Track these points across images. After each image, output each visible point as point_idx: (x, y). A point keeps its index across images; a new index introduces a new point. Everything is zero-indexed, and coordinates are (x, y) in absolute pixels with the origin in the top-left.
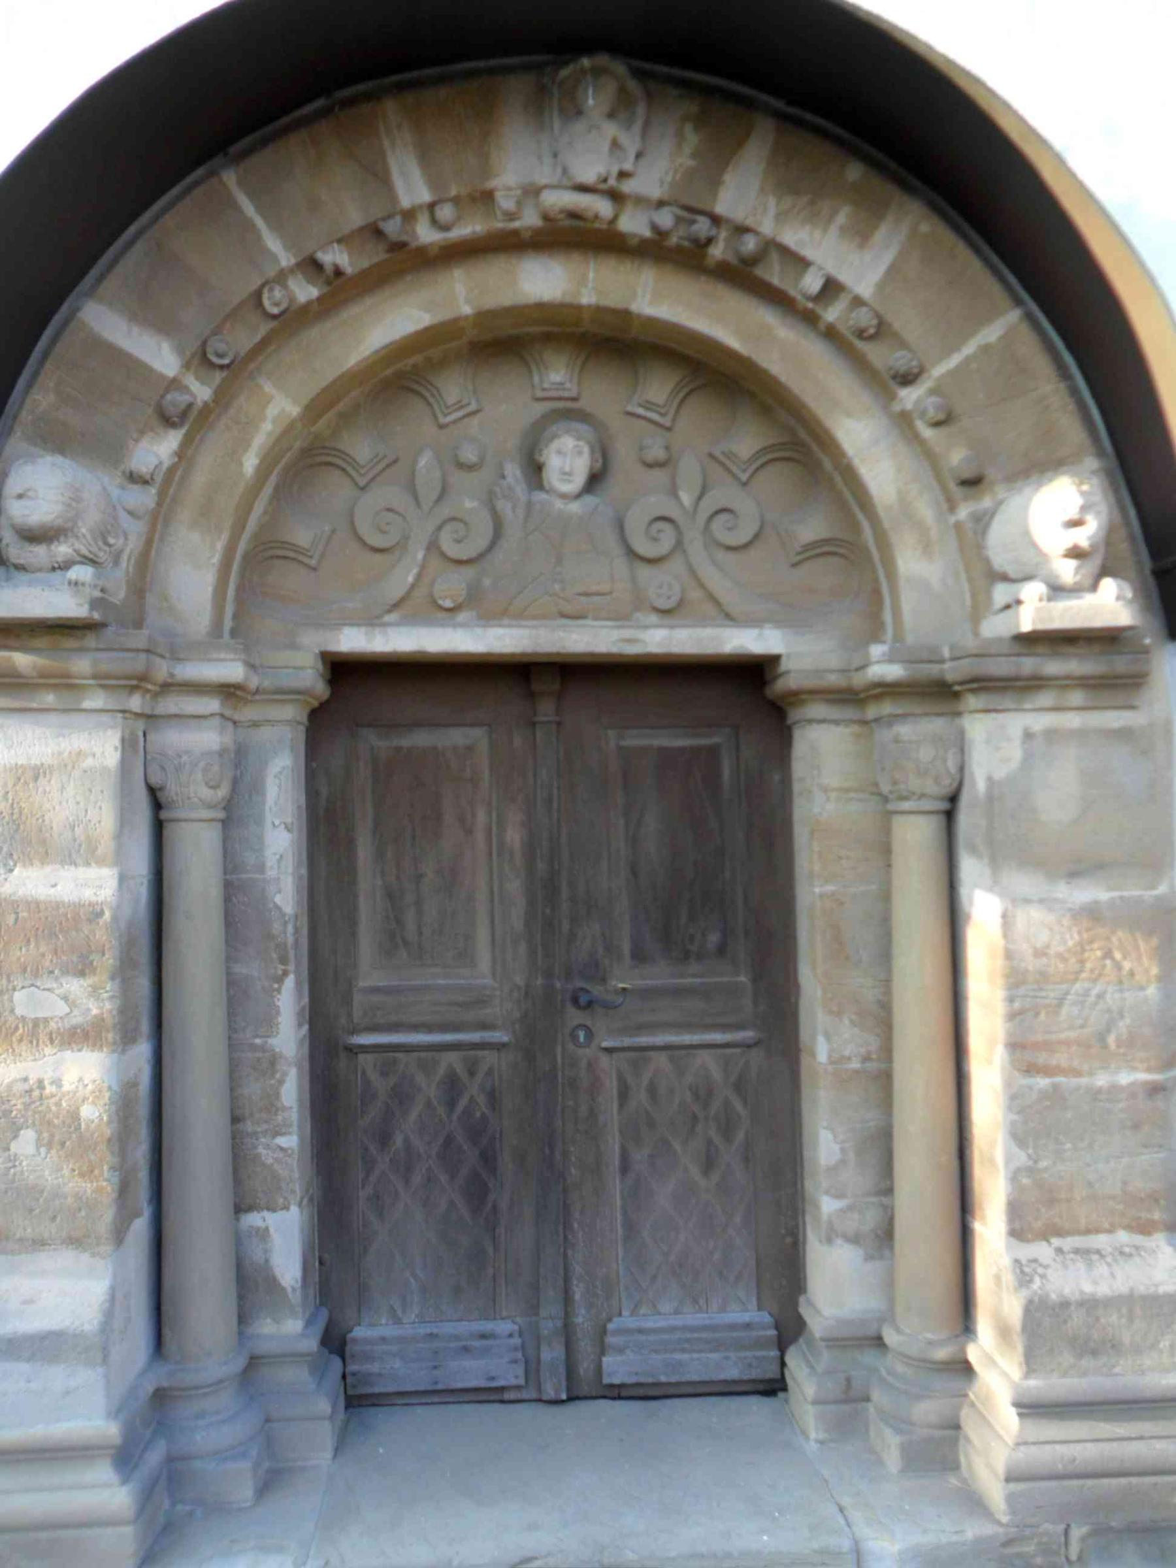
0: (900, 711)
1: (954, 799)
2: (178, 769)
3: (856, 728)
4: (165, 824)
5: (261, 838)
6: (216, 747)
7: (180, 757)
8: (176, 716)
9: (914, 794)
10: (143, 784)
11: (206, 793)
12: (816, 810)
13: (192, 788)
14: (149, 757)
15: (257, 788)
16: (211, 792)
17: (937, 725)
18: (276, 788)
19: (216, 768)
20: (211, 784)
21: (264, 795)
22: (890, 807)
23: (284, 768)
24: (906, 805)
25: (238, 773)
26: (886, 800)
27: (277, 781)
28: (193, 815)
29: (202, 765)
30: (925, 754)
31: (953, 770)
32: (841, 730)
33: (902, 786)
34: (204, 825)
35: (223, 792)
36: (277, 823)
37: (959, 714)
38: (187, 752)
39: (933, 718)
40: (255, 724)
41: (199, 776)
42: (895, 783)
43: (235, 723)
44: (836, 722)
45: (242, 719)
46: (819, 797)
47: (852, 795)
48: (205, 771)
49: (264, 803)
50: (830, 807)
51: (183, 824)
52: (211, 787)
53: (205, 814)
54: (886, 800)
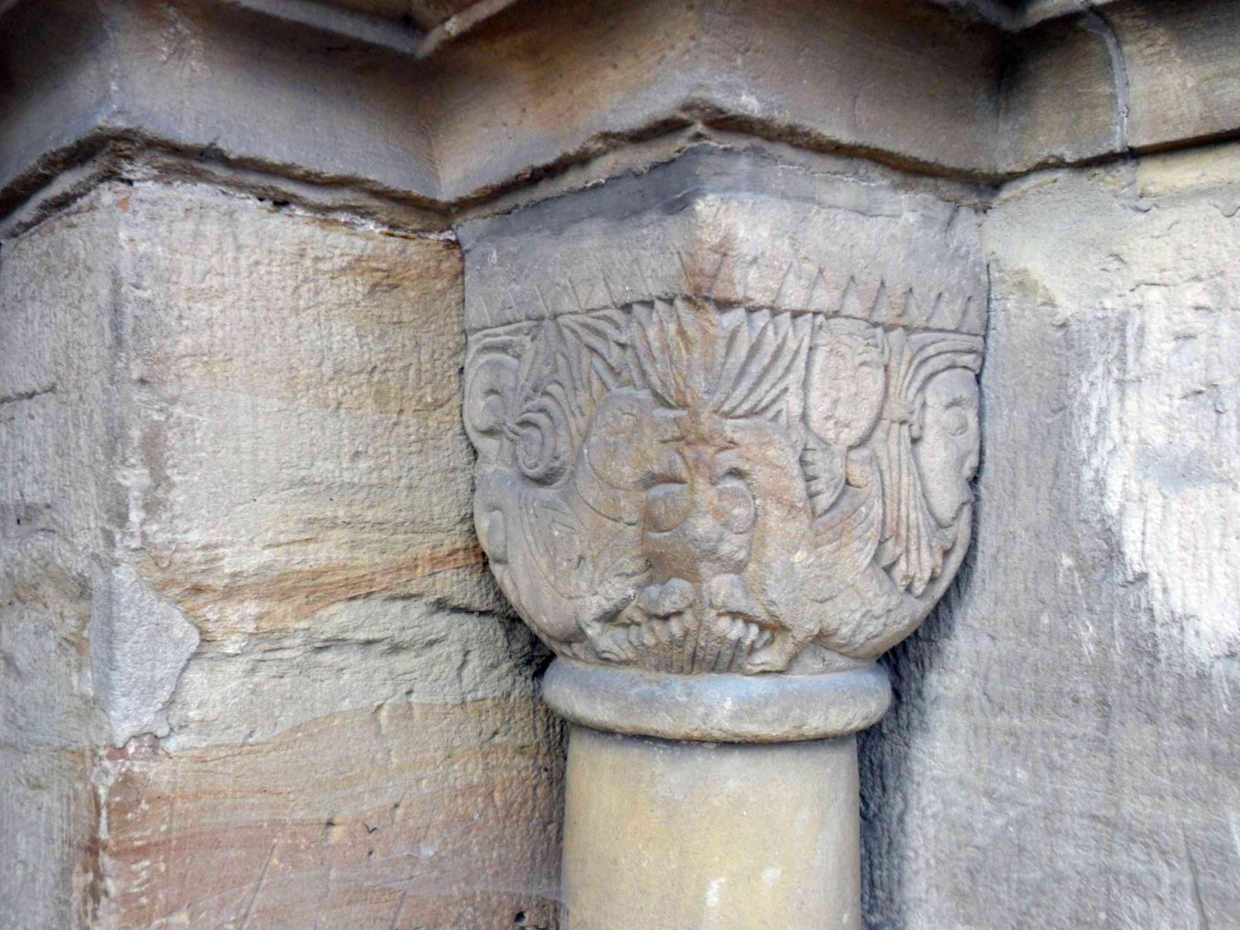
0: (749, 104)
1: (902, 661)
3: (368, 237)
9: (774, 628)
12: (126, 719)
17: (879, 231)
22: (566, 692)
24: (721, 702)
26: (537, 656)
30: (836, 390)
31: (947, 496)
32: (292, 228)
33: (721, 586)
37: (987, 185)
39: (880, 181)
42: (657, 566)
44: (276, 185)
46: (150, 631)
47: (338, 617)
50: (213, 692)
54: (537, 656)
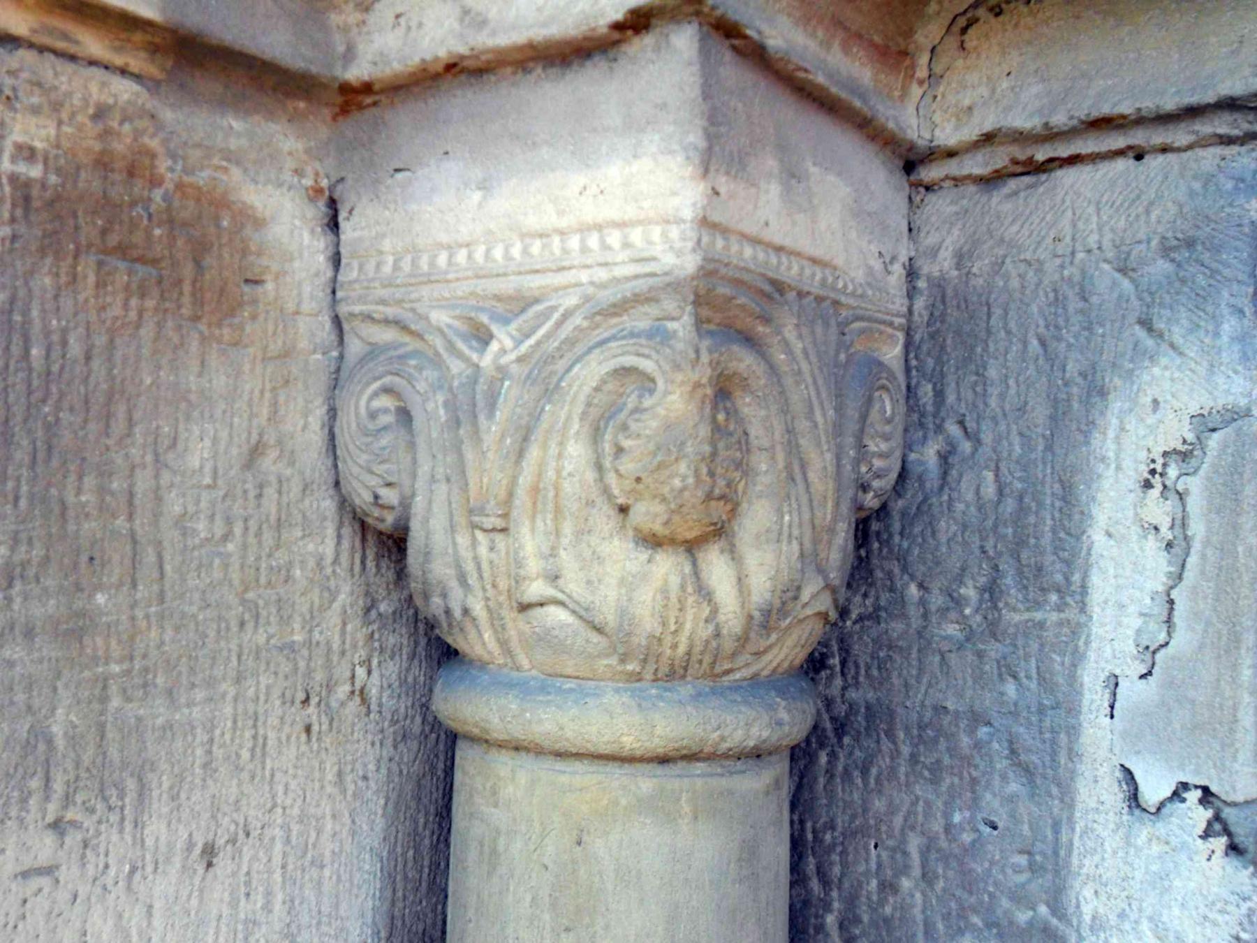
2: (468, 408)
4: (465, 754)
5: (1051, 866)
6: (673, 252)
7: (483, 338)
8: (453, 68)
10: (329, 506)
11: (627, 582)
13: (529, 542)
14: (355, 347)
15: (1039, 555)
16: (667, 567)
18: (1157, 565)
19: (674, 402)
20: (647, 513)
21: (1073, 593)
23: (1205, 424)
25: (929, 454)
27: (1158, 510)
28: (551, 720)
29: (589, 374)
34: (646, 782)
35: (764, 567)
36: (1154, 789)
38: (520, 304)
40: (1031, 159)
41: (569, 458)
43: (911, 161)
45: (948, 136)
48: (603, 421)
49: (1073, 640)
51: (503, 763)
52: (653, 542)
53: (618, 718)
